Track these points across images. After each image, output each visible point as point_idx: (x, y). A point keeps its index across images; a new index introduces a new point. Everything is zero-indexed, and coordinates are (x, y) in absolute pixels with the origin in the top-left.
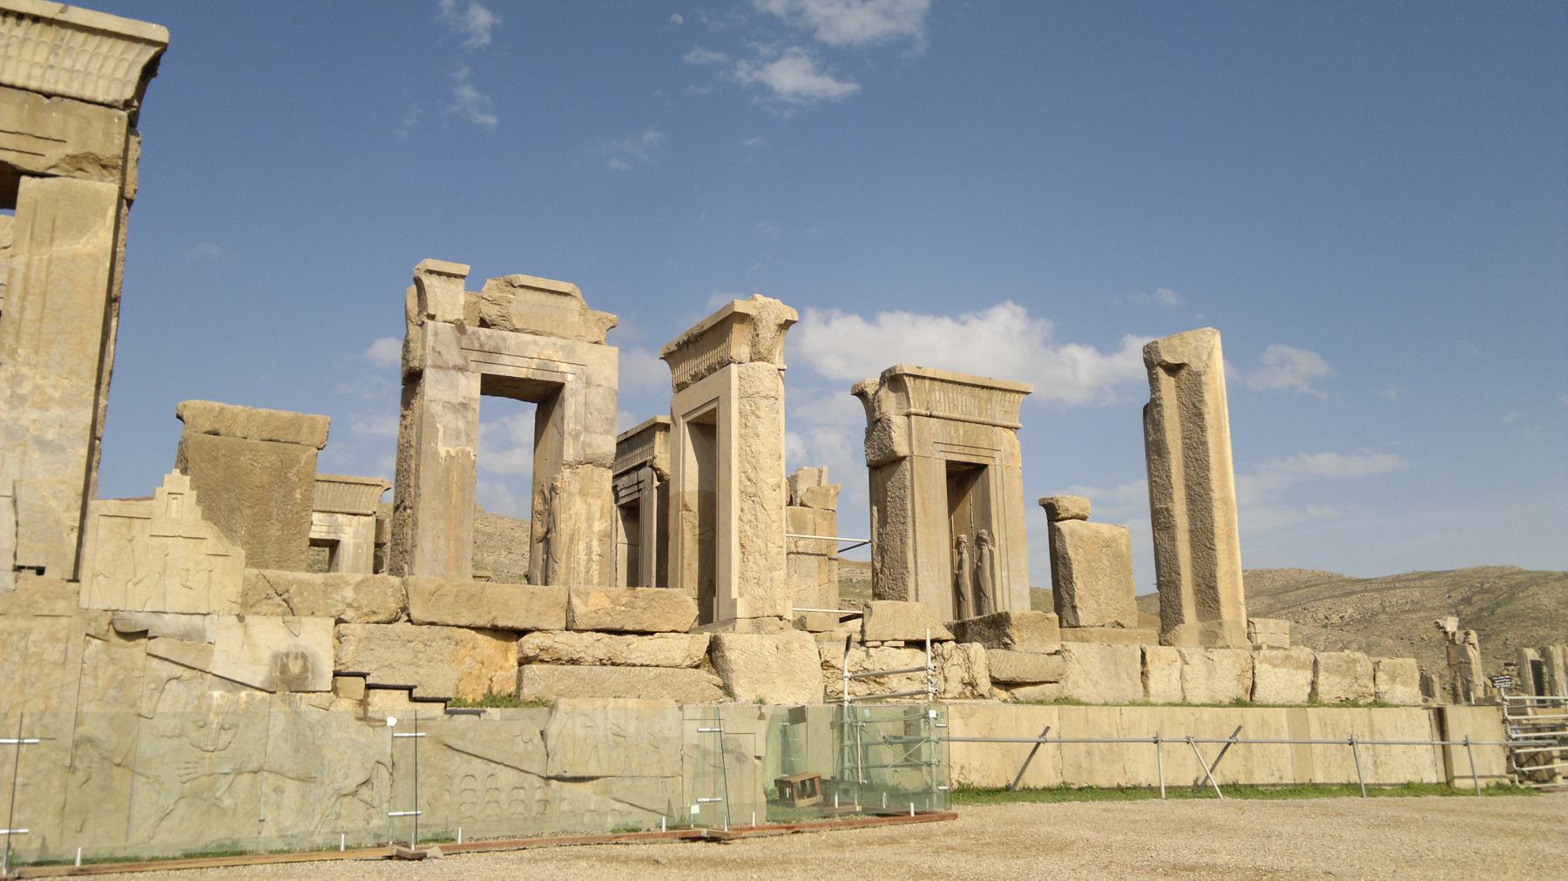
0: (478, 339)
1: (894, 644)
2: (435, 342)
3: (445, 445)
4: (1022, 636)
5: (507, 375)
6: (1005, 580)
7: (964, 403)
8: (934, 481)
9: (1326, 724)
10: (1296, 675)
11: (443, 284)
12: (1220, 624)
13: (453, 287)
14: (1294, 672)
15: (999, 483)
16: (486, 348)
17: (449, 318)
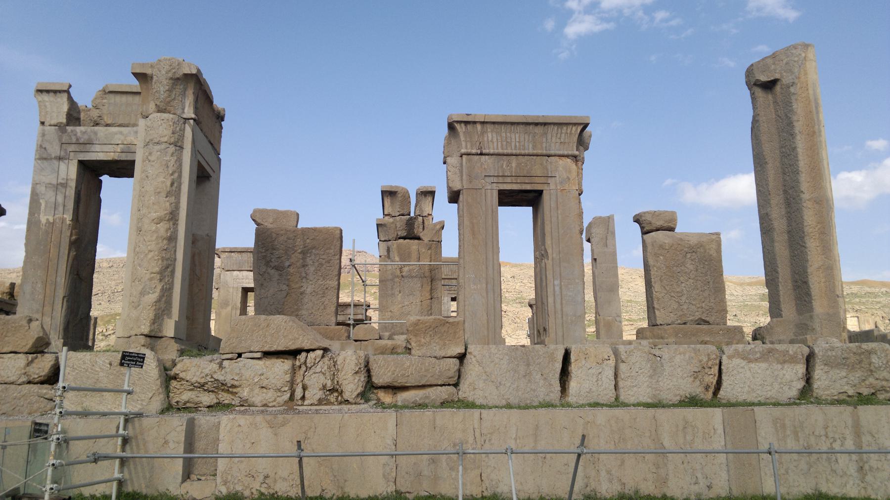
0: (75, 135)
1: (251, 355)
2: (42, 141)
3: (45, 215)
4: (420, 341)
5: (98, 159)
6: (557, 288)
7: (518, 140)
8: (484, 209)
9: (784, 426)
10: (782, 369)
11: (52, 99)
12: (811, 317)
13: (59, 100)
14: (780, 366)
15: (553, 205)
16: (81, 141)
17: (53, 122)
